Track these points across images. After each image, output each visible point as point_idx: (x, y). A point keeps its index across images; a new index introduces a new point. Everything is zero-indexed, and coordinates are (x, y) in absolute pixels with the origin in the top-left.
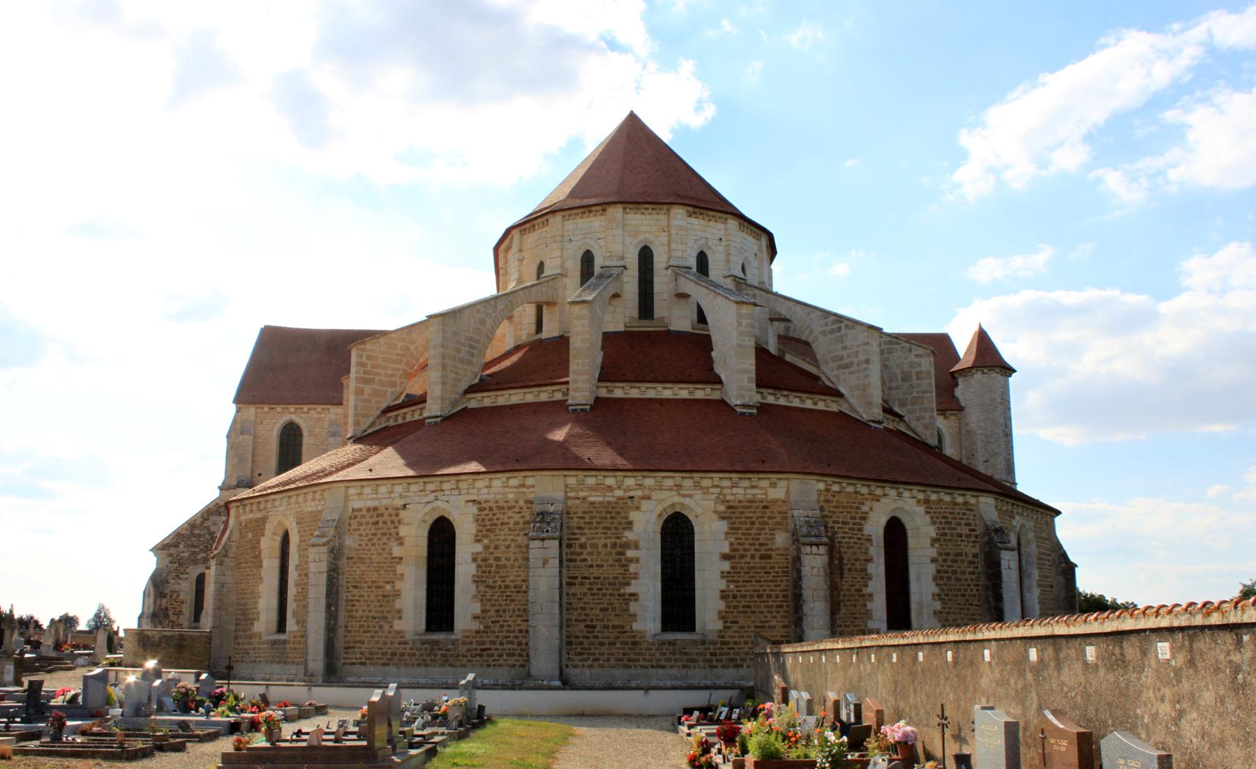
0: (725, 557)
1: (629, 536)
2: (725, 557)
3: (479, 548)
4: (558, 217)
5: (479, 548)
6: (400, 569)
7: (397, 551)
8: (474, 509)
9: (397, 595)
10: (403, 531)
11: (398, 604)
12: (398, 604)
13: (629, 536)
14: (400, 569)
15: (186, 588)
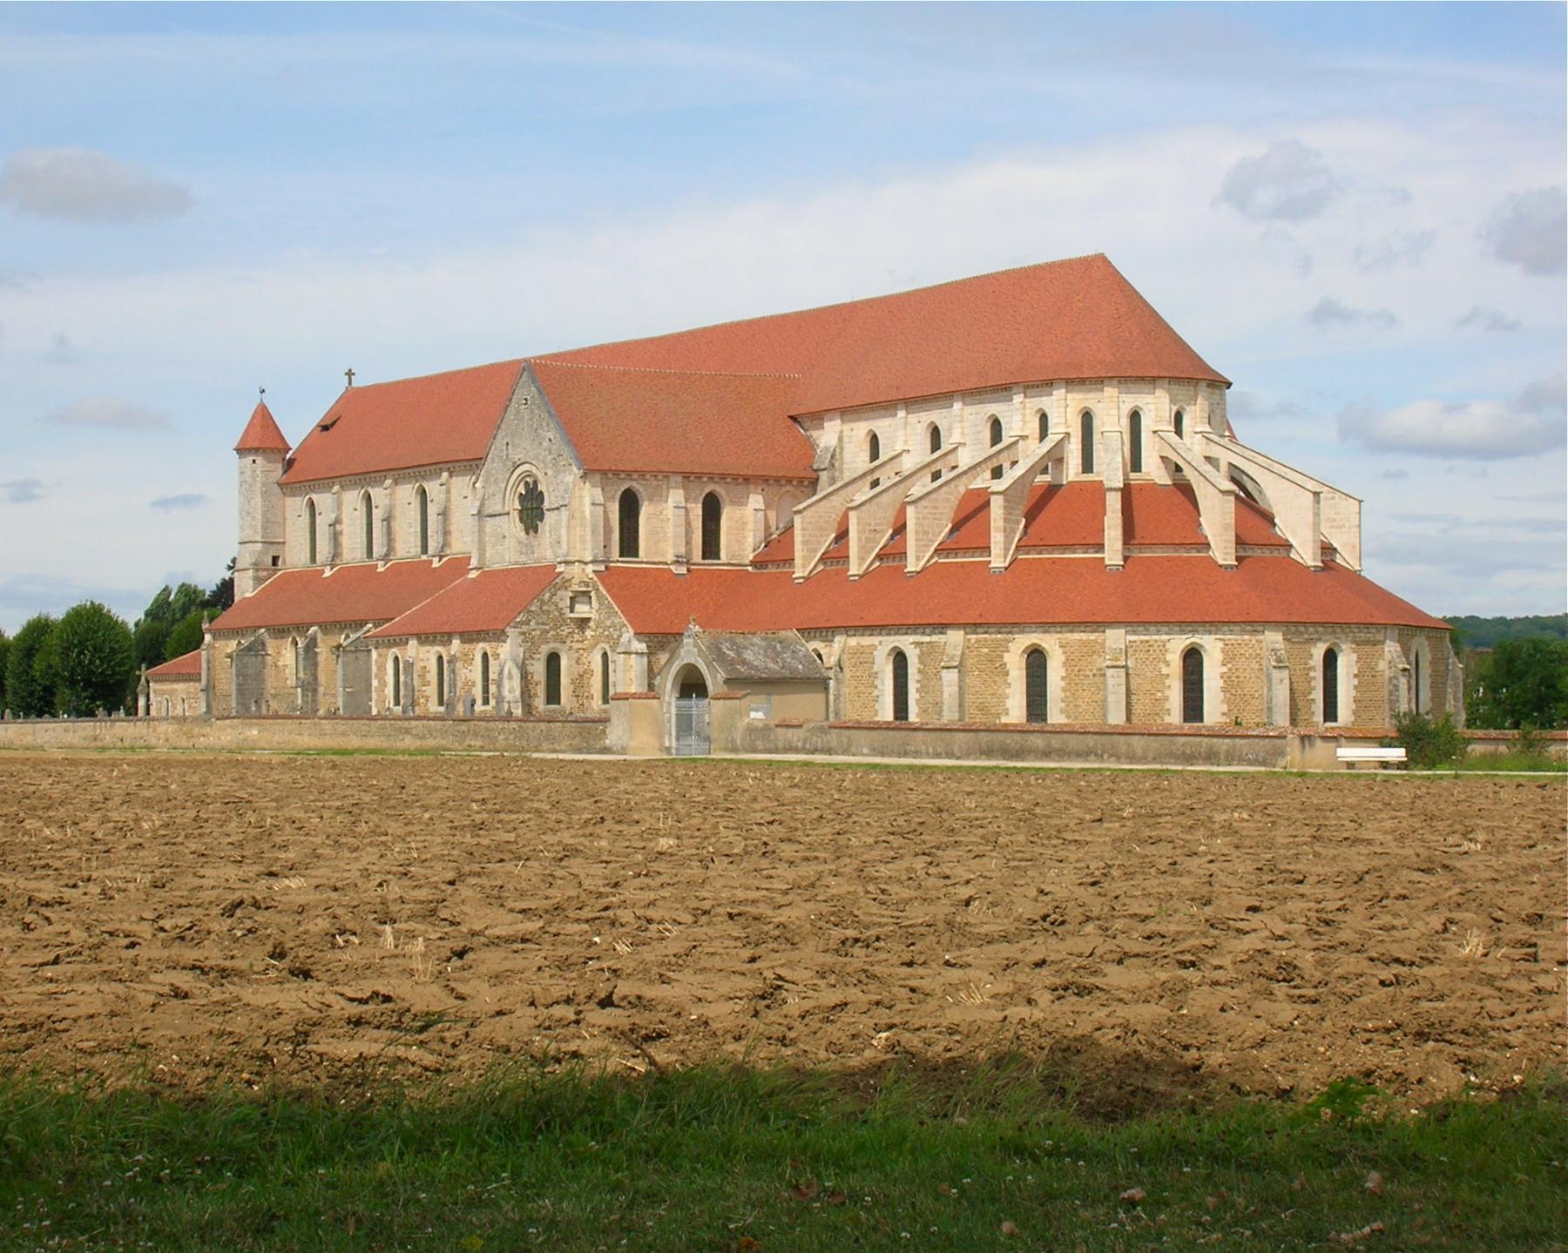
0: (1356, 676)
1: (1312, 663)
2: (1356, 676)
3: (1225, 669)
4: (1115, 382)
5: (1225, 669)
6: (1167, 682)
7: (1165, 671)
8: (1221, 644)
9: (1167, 699)
10: (1169, 657)
11: (1167, 706)
12: (1167, 706)
13: (1312, 663)
14: (1167, 682)
15: (538, 669)
